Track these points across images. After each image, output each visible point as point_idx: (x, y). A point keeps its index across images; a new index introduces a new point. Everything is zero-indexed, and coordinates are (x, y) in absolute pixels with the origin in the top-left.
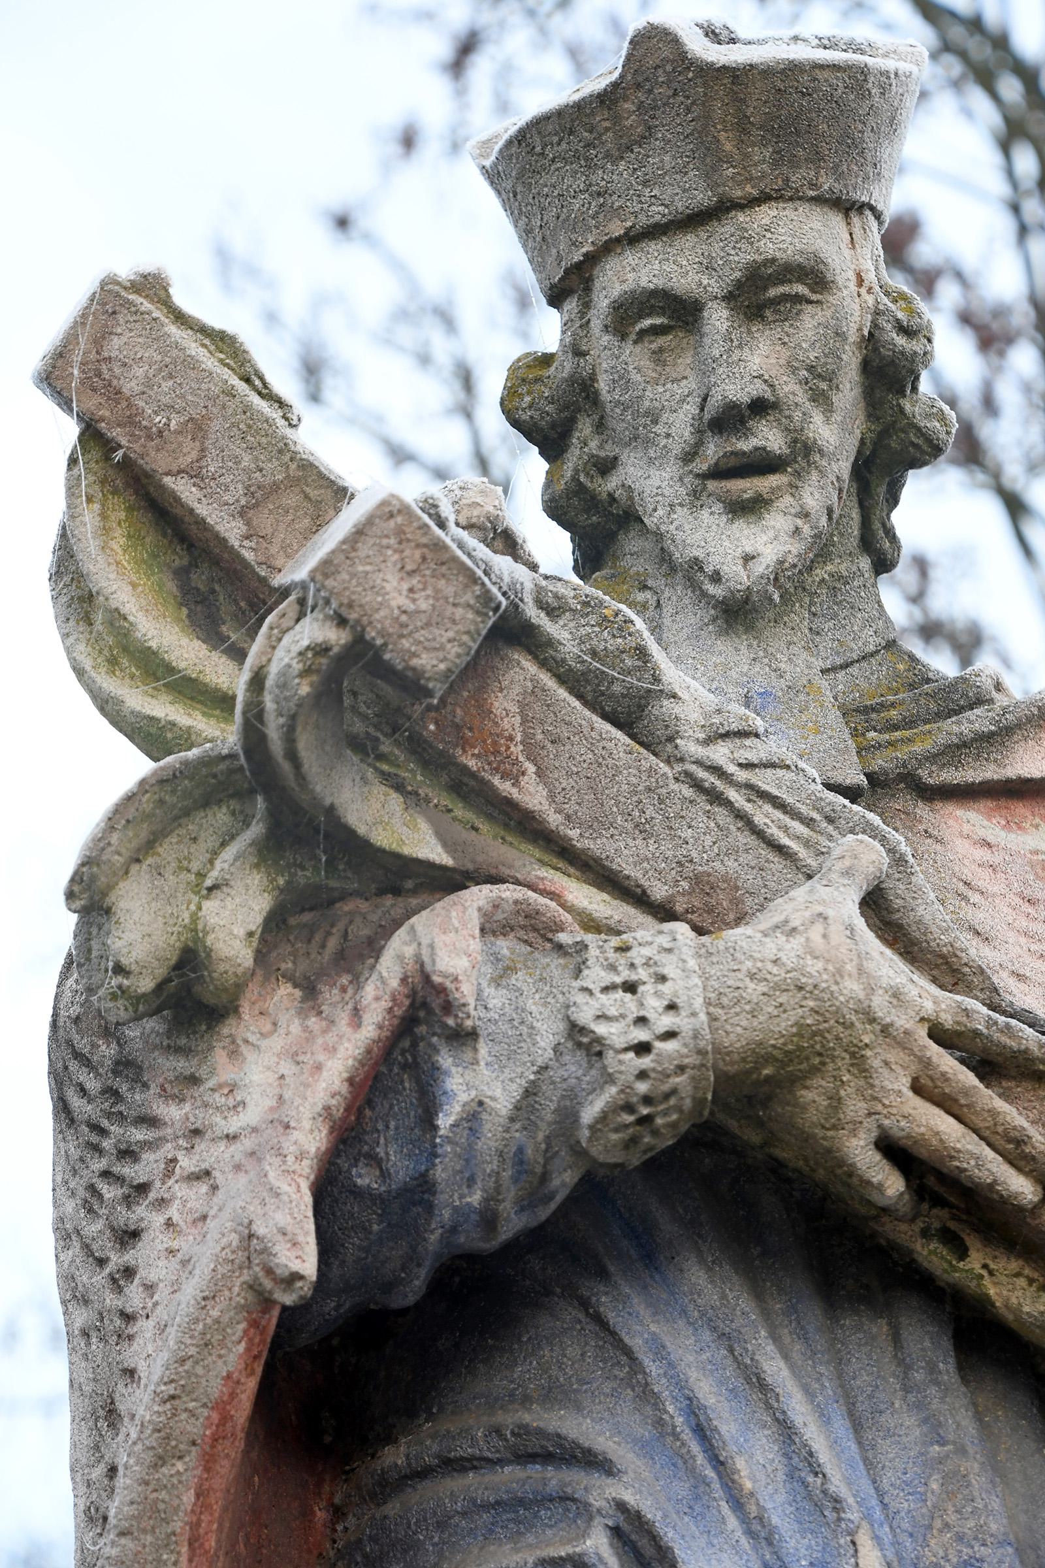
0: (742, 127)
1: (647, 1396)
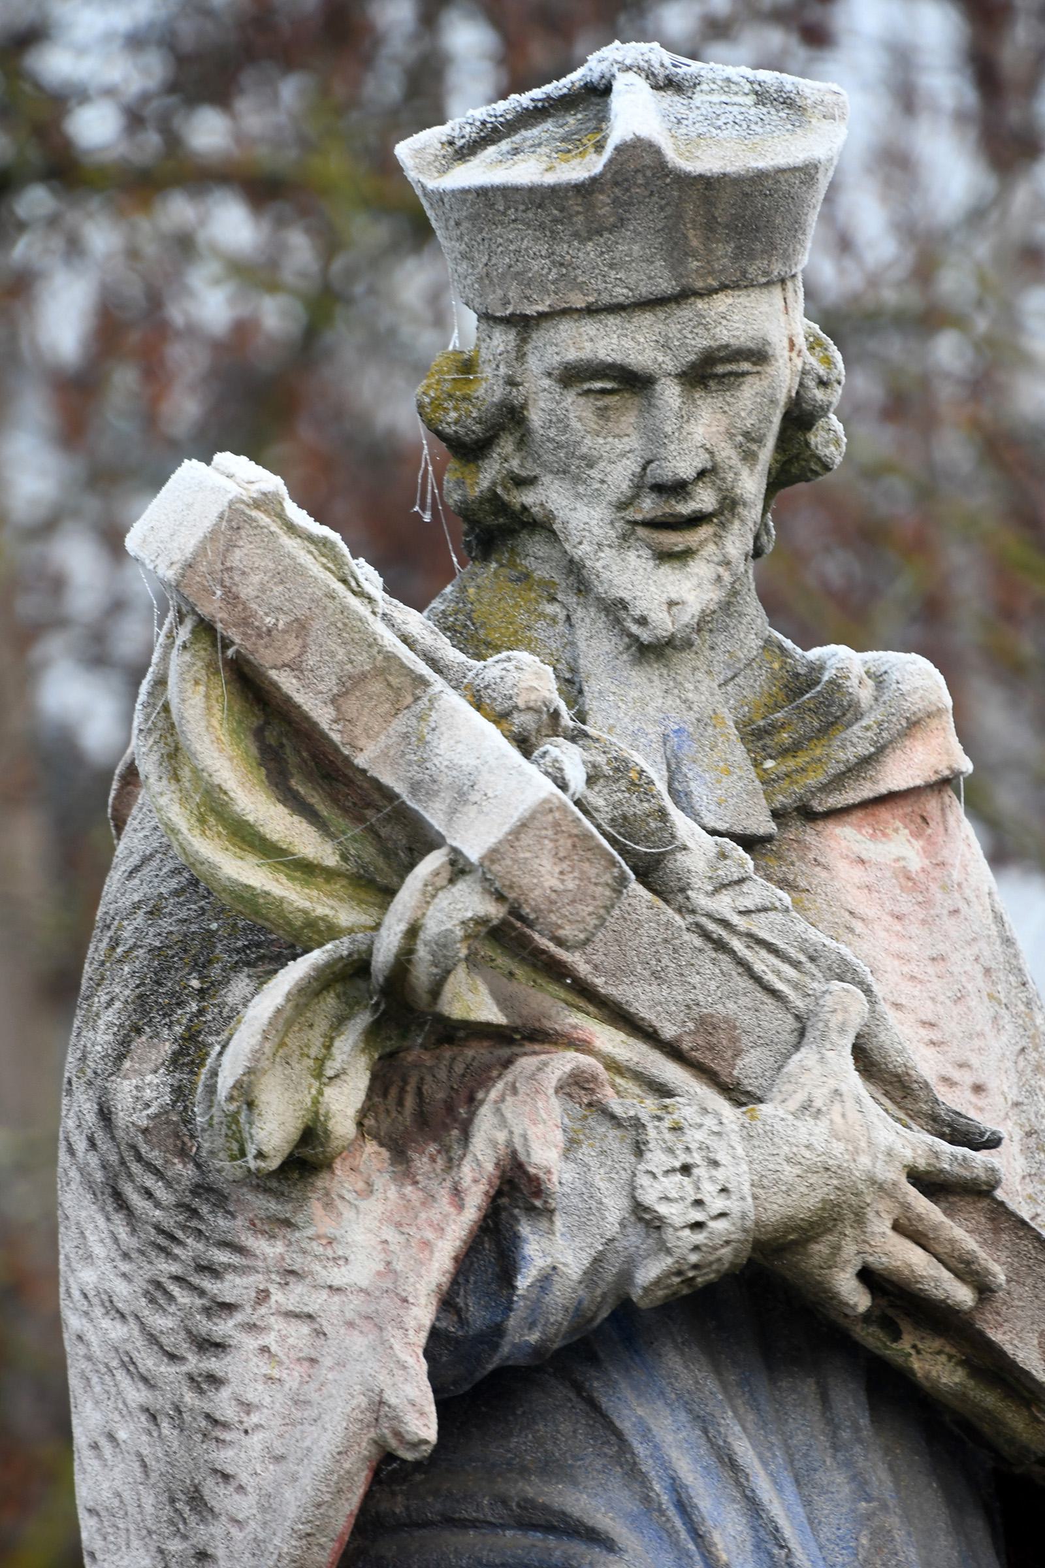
0: (710, 226)
1: (634, 1474)
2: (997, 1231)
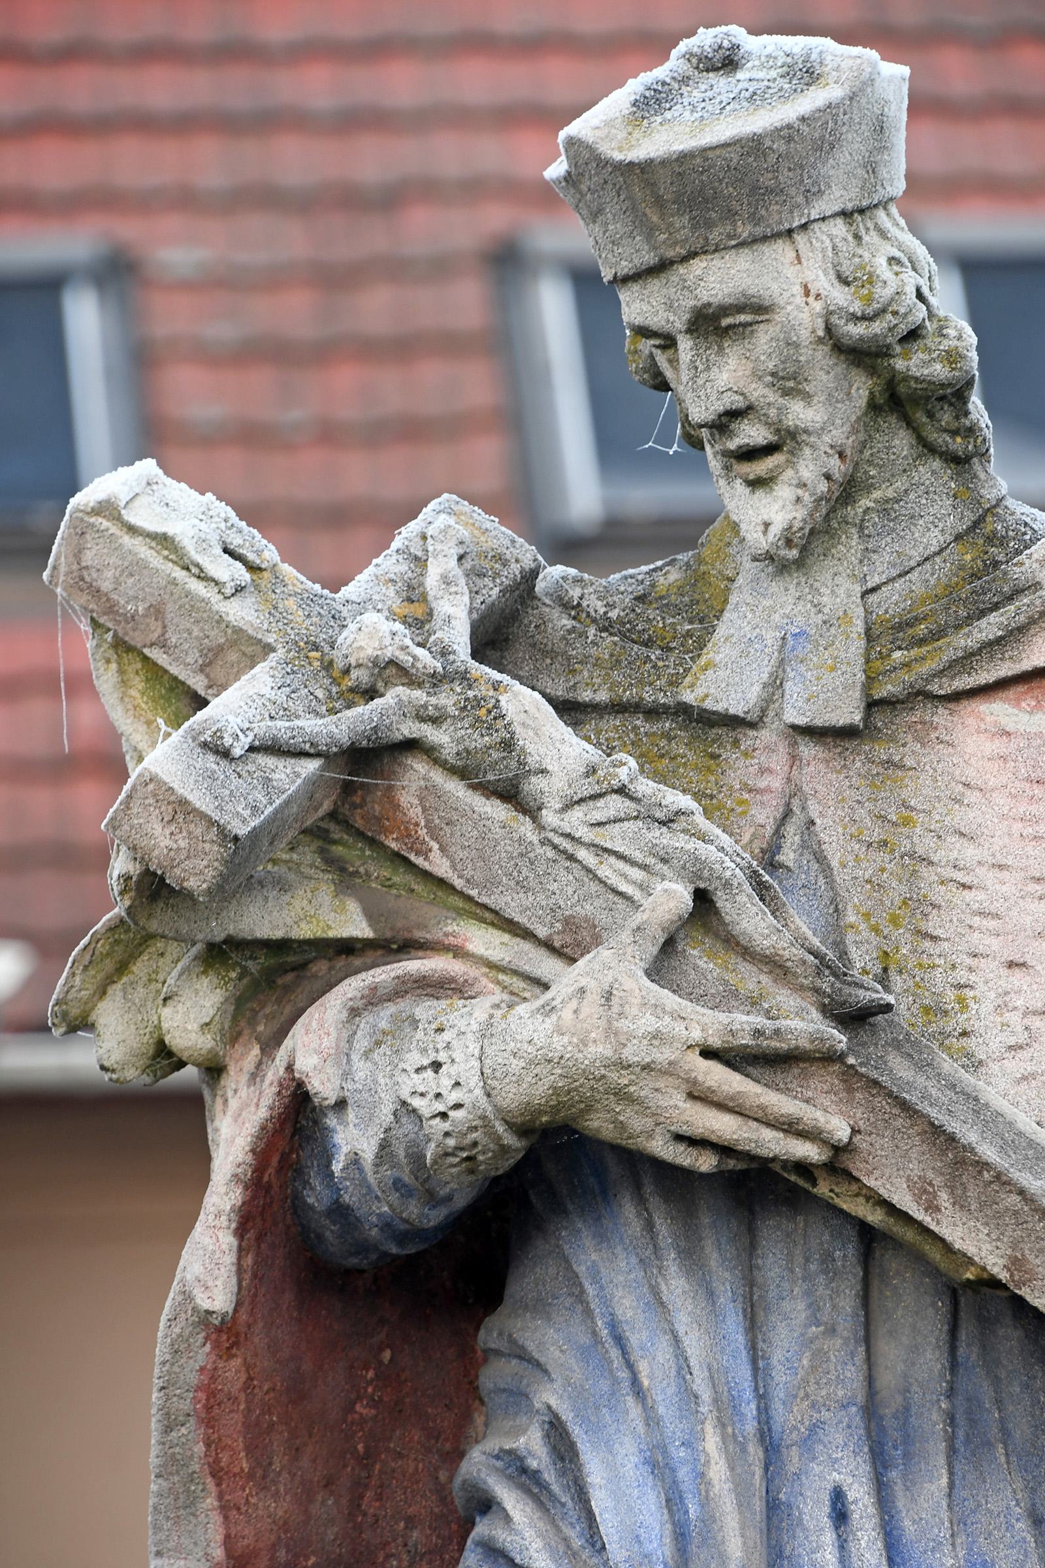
1: (588, 1313)
2: (850, 1090)
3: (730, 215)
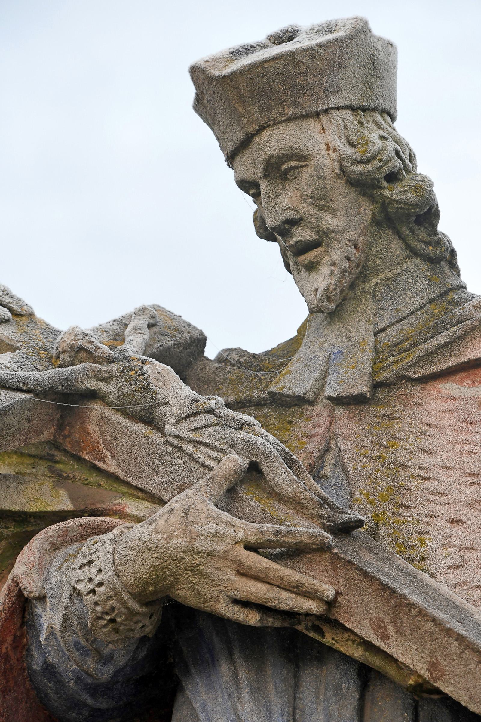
0: (242, 99)
2: (335, 569)
3: (281, 102)
